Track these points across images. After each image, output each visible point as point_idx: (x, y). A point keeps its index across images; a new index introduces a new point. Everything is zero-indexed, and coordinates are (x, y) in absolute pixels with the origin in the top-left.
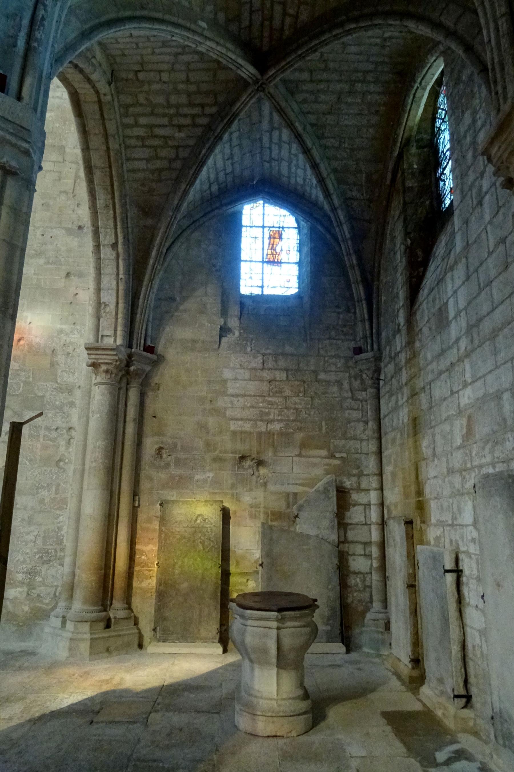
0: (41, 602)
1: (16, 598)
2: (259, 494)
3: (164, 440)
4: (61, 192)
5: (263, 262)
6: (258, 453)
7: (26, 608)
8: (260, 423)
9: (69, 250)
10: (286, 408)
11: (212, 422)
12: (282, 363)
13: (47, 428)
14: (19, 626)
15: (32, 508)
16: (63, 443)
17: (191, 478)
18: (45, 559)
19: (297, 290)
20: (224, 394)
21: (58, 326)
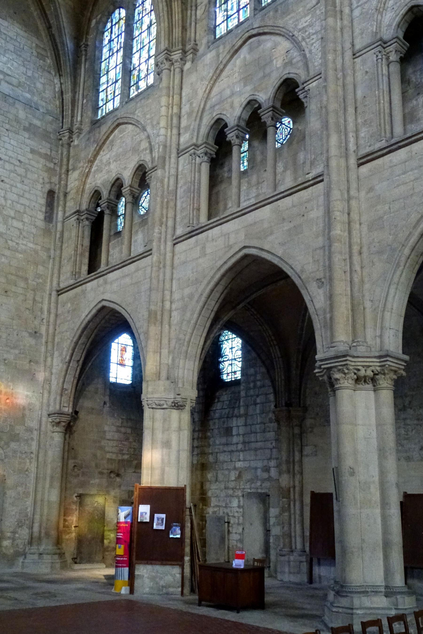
0: (18, 548)
1: (7, 546)
2: (117, 490)
3: (76, 461)
4: (27, 309)
5: (118, 364)
6: (118, 470)
7: (12, 551)
8: (120, 455)
9: (31, 346)
10: (131, 448)
11: (99, 453)
12: (130, 424)
13: (21, 453)
14: (9, 560)
15: (14, 497)
16: (28, 461)
17: (89, 482)
18: (20, 525)
19: (131, 382)
20: (104, 439)
21: (26, 393)
